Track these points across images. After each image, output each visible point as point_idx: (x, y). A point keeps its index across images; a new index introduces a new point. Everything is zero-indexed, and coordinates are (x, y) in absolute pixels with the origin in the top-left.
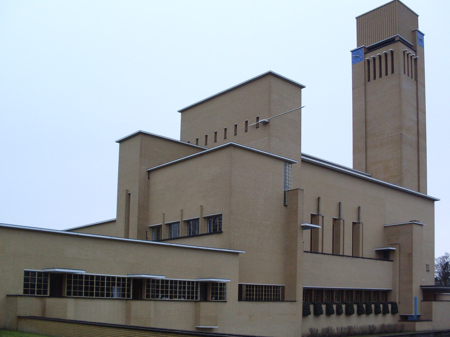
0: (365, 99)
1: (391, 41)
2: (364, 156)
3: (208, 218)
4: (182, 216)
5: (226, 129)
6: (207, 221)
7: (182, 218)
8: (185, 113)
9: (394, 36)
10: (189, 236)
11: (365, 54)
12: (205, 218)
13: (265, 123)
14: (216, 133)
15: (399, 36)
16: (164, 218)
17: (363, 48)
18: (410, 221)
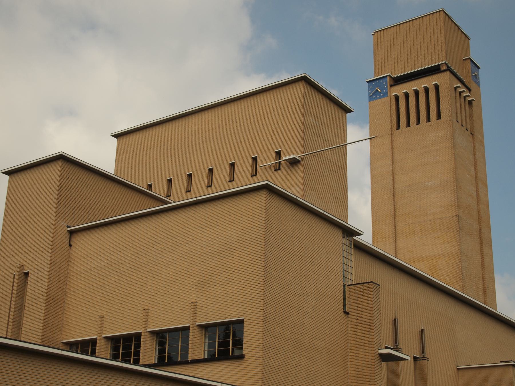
0: (393, 156)
1: (435, 70)
2: (394, 247)
3: (205, 328)
4: (146, 321)
5: (211, 171)
6: (155, 339)
7: (146, 327)
8: (125, 140)
9: (439, 63)
10: (211, 359)
11: (391, 86)
12: (201, 327)
13: (294, 163)
14: (190, 176)
15: (446, 64)
16: (102, 325)
17: (388, 78)
18: (501, 362)
